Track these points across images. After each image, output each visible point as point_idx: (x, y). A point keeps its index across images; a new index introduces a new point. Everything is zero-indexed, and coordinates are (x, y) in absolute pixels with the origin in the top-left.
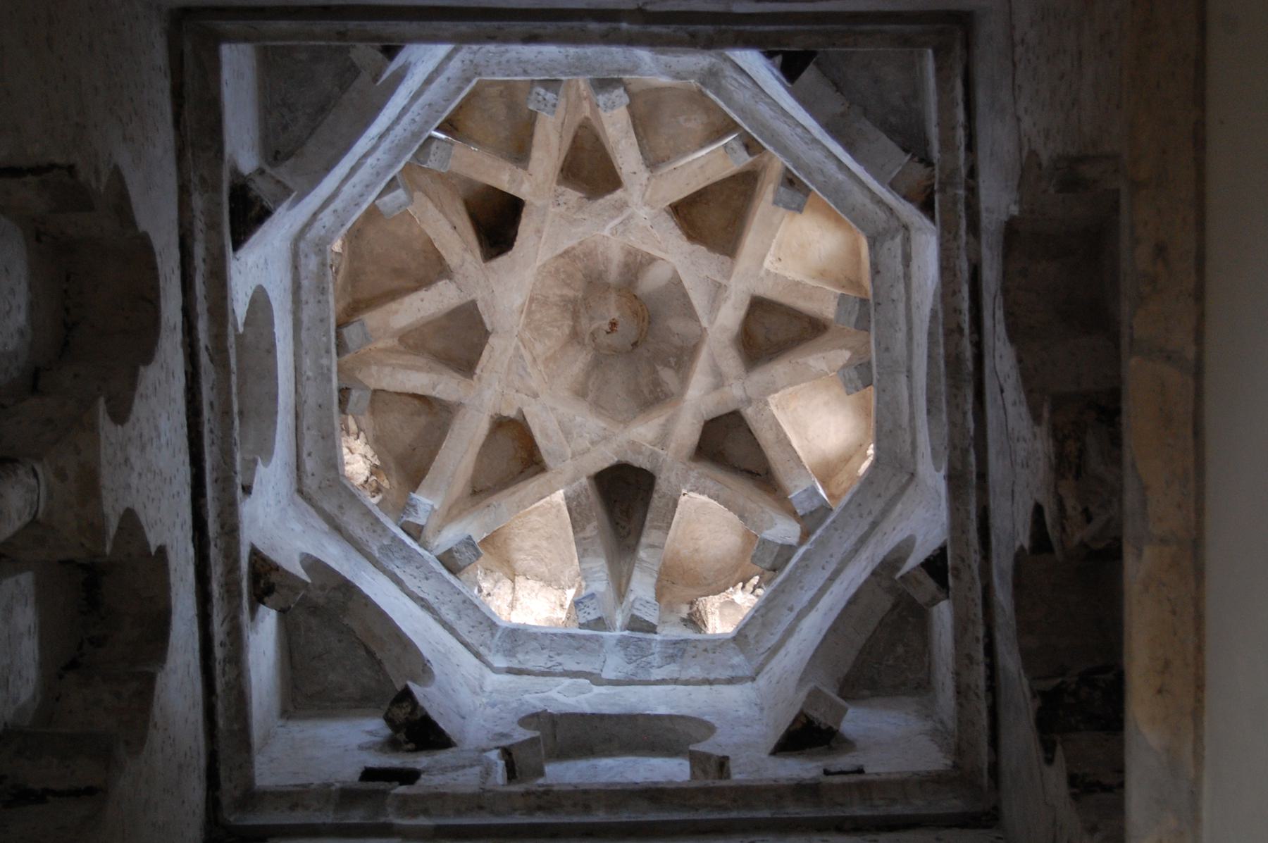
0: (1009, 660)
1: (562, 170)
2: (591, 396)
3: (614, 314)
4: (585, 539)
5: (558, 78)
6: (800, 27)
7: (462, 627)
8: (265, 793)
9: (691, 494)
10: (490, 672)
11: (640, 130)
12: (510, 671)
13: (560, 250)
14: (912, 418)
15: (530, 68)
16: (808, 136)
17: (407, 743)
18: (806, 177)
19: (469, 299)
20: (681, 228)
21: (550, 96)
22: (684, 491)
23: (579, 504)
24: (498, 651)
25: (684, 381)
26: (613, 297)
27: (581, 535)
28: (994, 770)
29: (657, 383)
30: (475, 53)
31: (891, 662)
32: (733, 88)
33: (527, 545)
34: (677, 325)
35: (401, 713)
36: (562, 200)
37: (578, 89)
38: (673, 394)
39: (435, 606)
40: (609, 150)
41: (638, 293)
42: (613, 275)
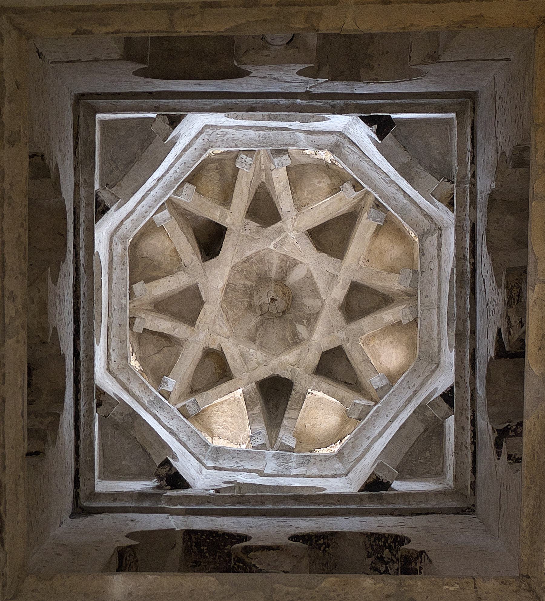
0: (483, 422)
1: (248, 212)
2: (258, 342)
3: (273, 295)
4: (253, 414)
5: (253, 149)
6: (388, 101)
7: (190, 445)
8: (100, 494)
9: (314, 392)
10: (205, 468)
11: (293, 188)
12: (214, 468)
13: (244, 258)
14: (439, 333)
15: (239, 144)
16: (389, 179)
17: (166, 486)
18: (386, 202)
19: (194, 282)
20: (314, 244)
21: (248, 159)
22: (309, 391)
23: (250, 397)
24: (208, 459)
25: (311, 333)
26: (273, 285)
27: (251, 412)
28: (474, 486)
29: (295, 334)
30: (210, 135)
31: (422, 461)
32: (348, 153)
33: (221, 420)
34: (310, 302)
35: (164, 471)
36: (248, 227)
37: (260, 162)
38: (304, 340)
39: (177, 433)
40: (275, 200)
41: (287, 284)
42: (273, 274)
